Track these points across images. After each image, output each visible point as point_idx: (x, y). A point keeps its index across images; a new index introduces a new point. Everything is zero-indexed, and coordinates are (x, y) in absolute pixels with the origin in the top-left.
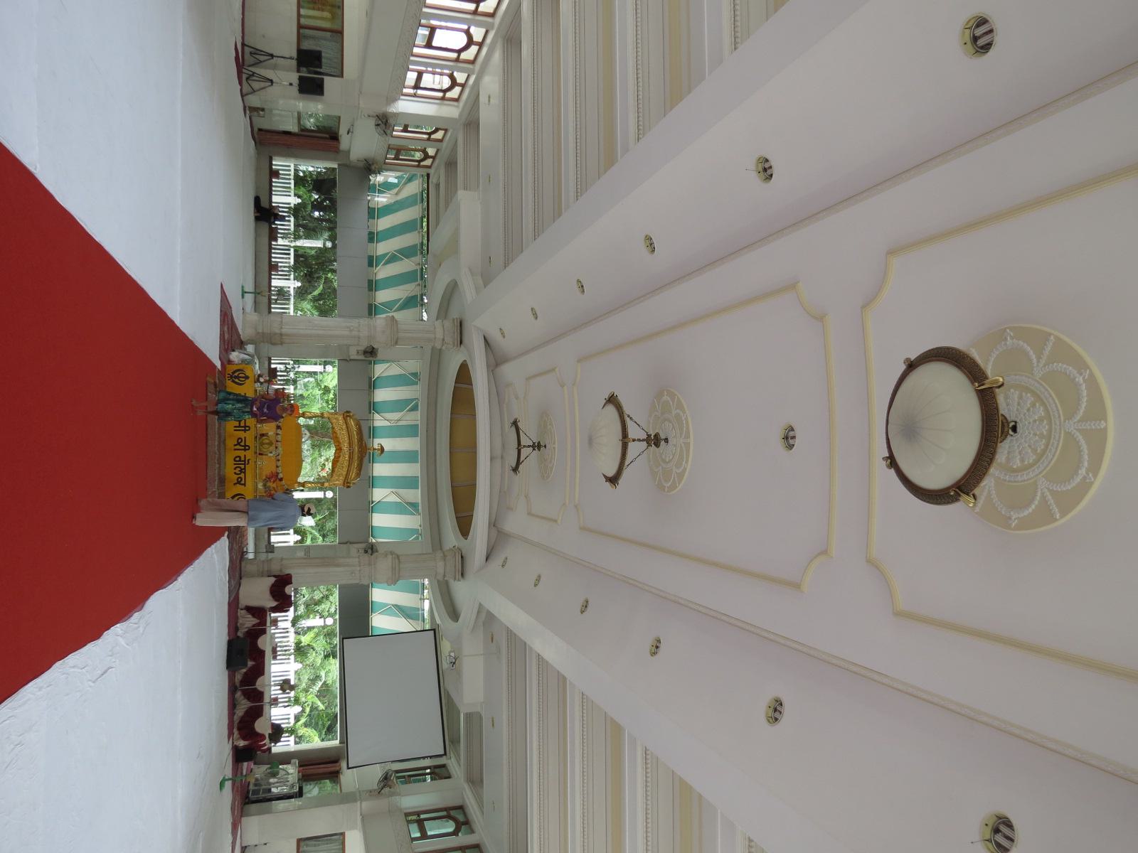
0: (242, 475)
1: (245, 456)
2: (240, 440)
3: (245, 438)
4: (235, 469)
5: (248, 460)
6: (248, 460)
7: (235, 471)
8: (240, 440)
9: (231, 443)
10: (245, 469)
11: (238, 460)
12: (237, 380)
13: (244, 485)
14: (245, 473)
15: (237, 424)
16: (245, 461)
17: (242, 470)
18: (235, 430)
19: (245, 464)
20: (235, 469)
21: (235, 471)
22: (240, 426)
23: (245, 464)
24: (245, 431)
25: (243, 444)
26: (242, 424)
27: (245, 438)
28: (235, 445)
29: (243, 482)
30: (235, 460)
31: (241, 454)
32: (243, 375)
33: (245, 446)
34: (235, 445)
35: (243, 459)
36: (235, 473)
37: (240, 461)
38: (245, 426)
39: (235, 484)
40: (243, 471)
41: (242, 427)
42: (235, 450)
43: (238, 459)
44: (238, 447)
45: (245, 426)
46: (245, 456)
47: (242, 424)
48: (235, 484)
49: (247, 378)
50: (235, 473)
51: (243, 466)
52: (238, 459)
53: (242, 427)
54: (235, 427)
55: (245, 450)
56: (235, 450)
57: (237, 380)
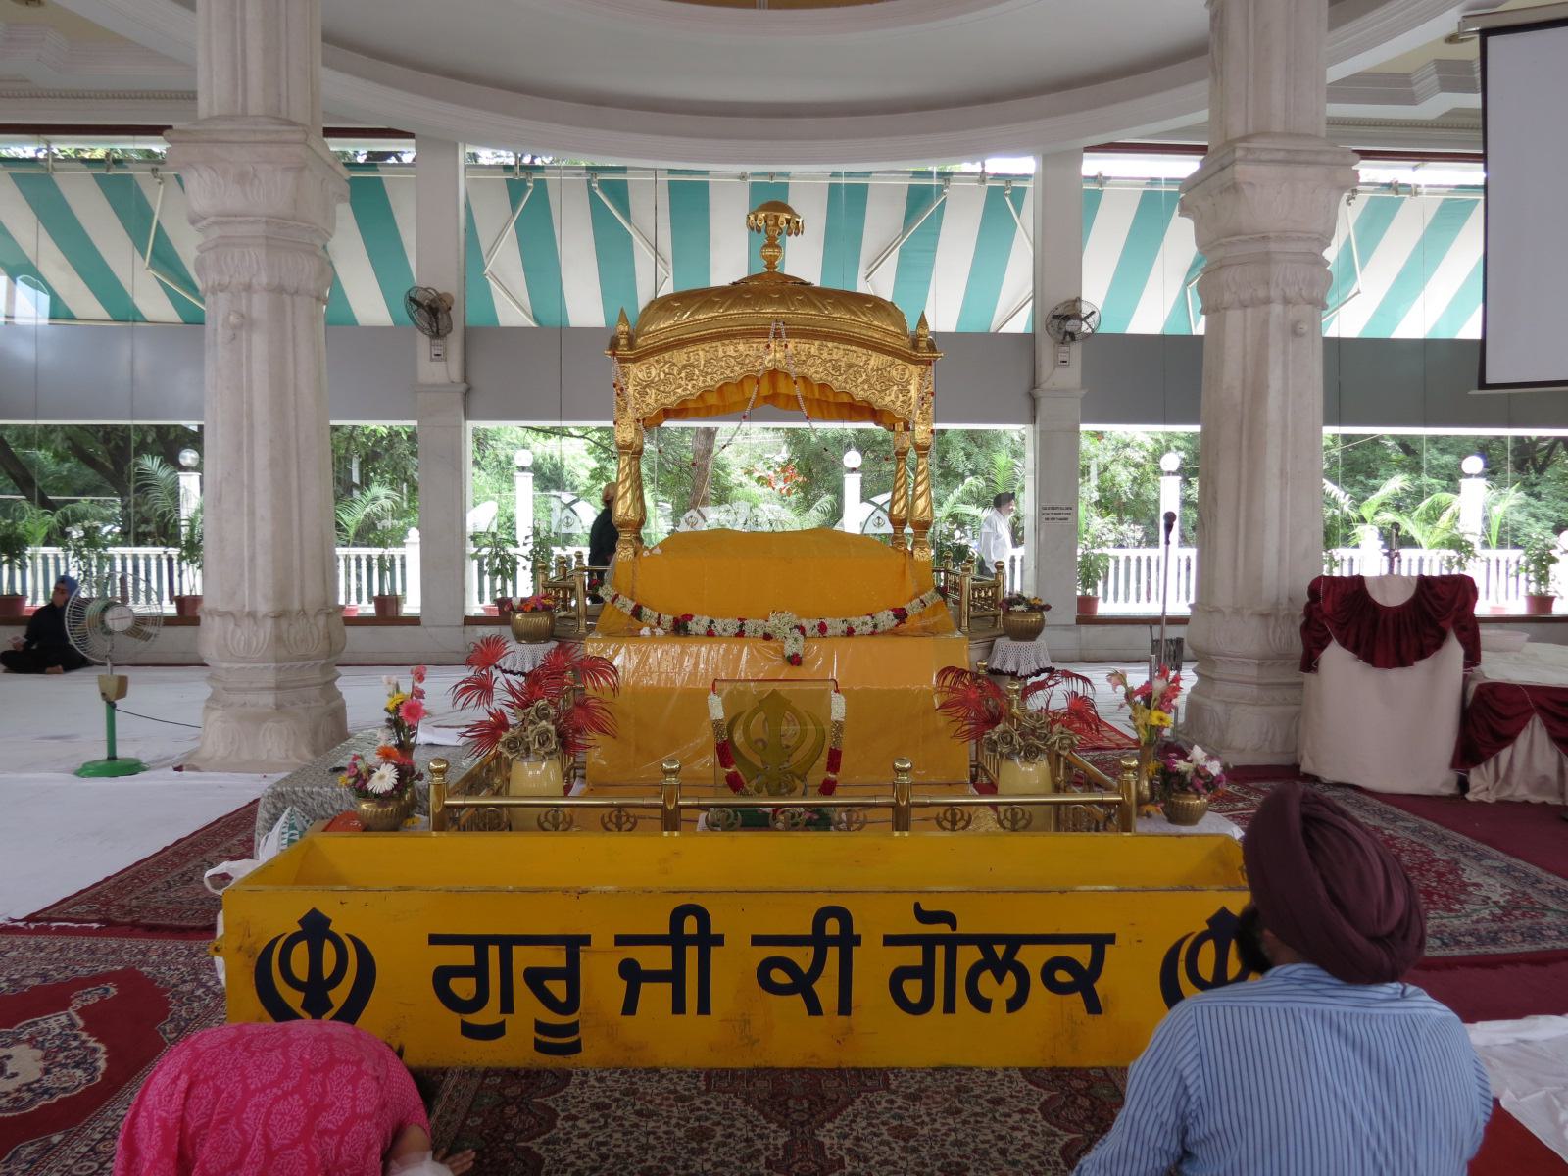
0: (1033, 958)
1: (890, 940)
2: (779, 976)
3: (758, 940)
4: (983, 1005)
5: (923, 916)
6: (923, 916)
7: (999, 1005)
8: (779, 976)
9: (791, 1036)
10: (985, 942)
11: (919, 988)
12: (339, 995)
13: (1100, 943)
14: (1015, 942)
15: (655, 996)
16: (928, 943)
17: (989, 962)
18: (704, 1008)
19: (952, 943)
20: (983, 1005)
21: (999, 1005)
22: (676, 976)
23: (952, 943)
24: (708, 940)
25: (803, 958)
26: (658, 958)
27: (758, 940)
28: (814, 1008)
29: (1082, 954)
30: (924, 1007)
31: (873, 965)
32: (301, 950)
33: (818, 940)
34: (814, 1008)
35: (913, 956)
36: (1015, 1003)
37: (925, 973)
38: (675, 939)
39: (1093, 1006)
40: (1000, 953)
41: (679, 959)
42: (845, 1007)
43: (913, 989)
44: (826, 988)
45: (675, 939)
46: (890, 940)
47: (658, 958)
48: (1093, 1006)
49: (315, 928)
50: (1015, 1003)
51: (969, 956)
52: (913, 989)
53: (679, 959)
54: (679, 1007)
55: (848, 940)
56: (845, 1007)
57: (339, 995)
